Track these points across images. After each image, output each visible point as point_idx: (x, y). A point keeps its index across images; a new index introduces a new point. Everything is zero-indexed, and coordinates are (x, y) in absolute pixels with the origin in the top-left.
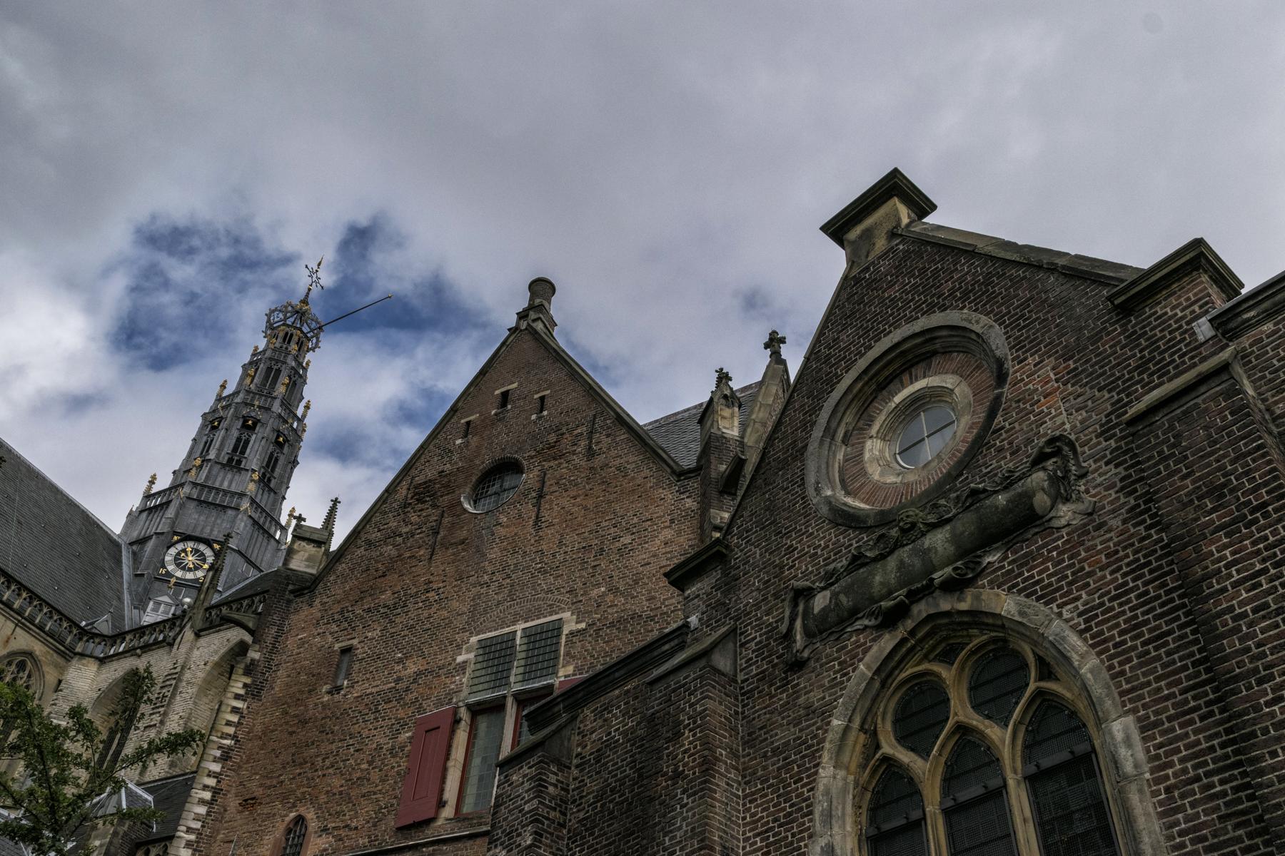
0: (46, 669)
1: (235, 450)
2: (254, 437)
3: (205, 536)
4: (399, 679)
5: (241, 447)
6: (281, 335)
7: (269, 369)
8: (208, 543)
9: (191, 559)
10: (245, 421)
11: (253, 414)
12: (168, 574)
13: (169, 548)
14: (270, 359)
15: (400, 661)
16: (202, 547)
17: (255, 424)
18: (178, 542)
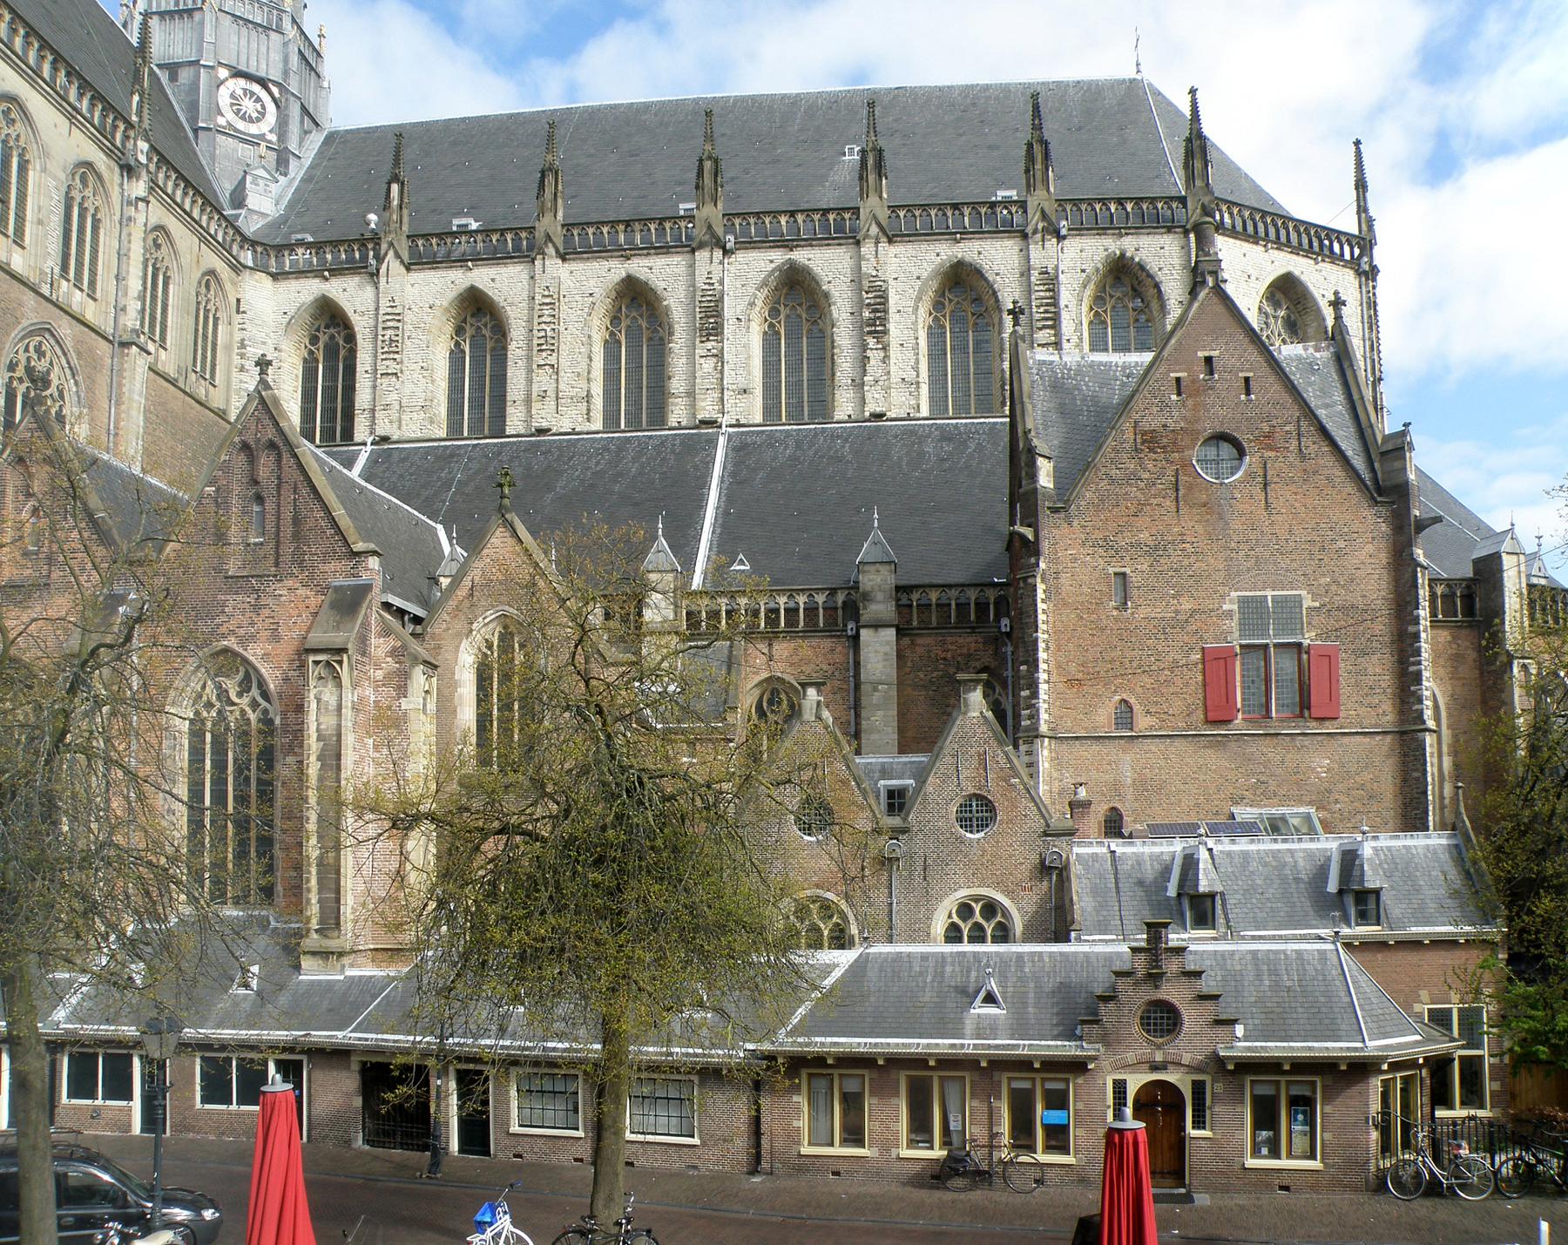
0: (228, 286)
3: (252, 70)
4: (1177, 612)
8: (263, 83)
9: (249, 106)
15: (1174, 597)
16: (256, 88)
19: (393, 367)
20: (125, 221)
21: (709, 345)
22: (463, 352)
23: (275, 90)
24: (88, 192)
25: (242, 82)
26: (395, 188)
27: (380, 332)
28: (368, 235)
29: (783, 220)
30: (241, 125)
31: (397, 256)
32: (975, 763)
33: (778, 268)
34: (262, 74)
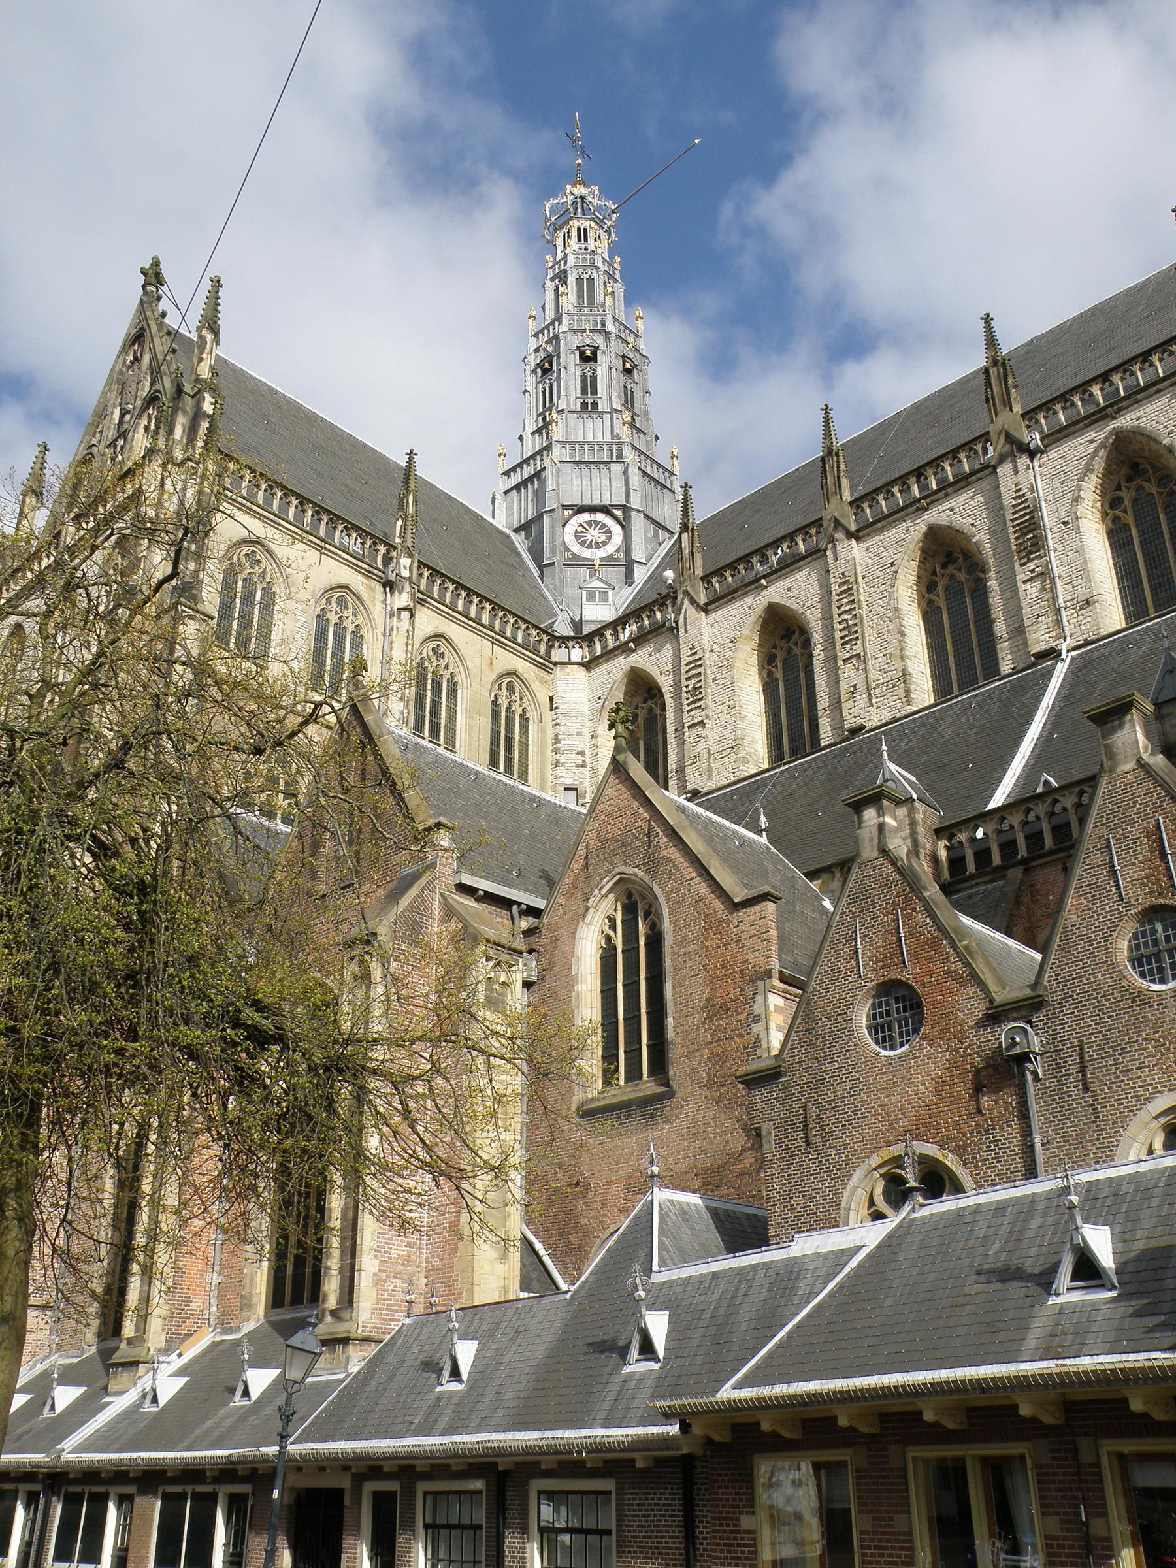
0: (535, 686)
1: (584, 391)
2: (599, 370)
3: (596, 502)
5: (589, 385)
6: (574, 233)
7: (579, 280)
8: (605, 510)
9: (594, 534)
10: (582, 354)
11: (588, 342)
12: (575, 557)
13: (564, 526)
14: (576, 267)
16: (600, 517)
17: (594, 353)
18: (571, 517)
19: (698, 715)
20: (389, 632)
21: (1032, 565)
22: (777, 679)
23: (619, 513)
24: (349, 613)
25: (586, 517)
26: (685, 536)
27: (684, 683)
28: (665, 591)
29: (1096, 390)
30: (587, 554)
31: (693, 602)
32: (1144, 850)
33: (1103, 445)
34: (606, 502)
